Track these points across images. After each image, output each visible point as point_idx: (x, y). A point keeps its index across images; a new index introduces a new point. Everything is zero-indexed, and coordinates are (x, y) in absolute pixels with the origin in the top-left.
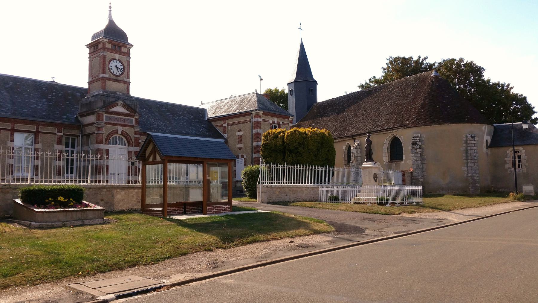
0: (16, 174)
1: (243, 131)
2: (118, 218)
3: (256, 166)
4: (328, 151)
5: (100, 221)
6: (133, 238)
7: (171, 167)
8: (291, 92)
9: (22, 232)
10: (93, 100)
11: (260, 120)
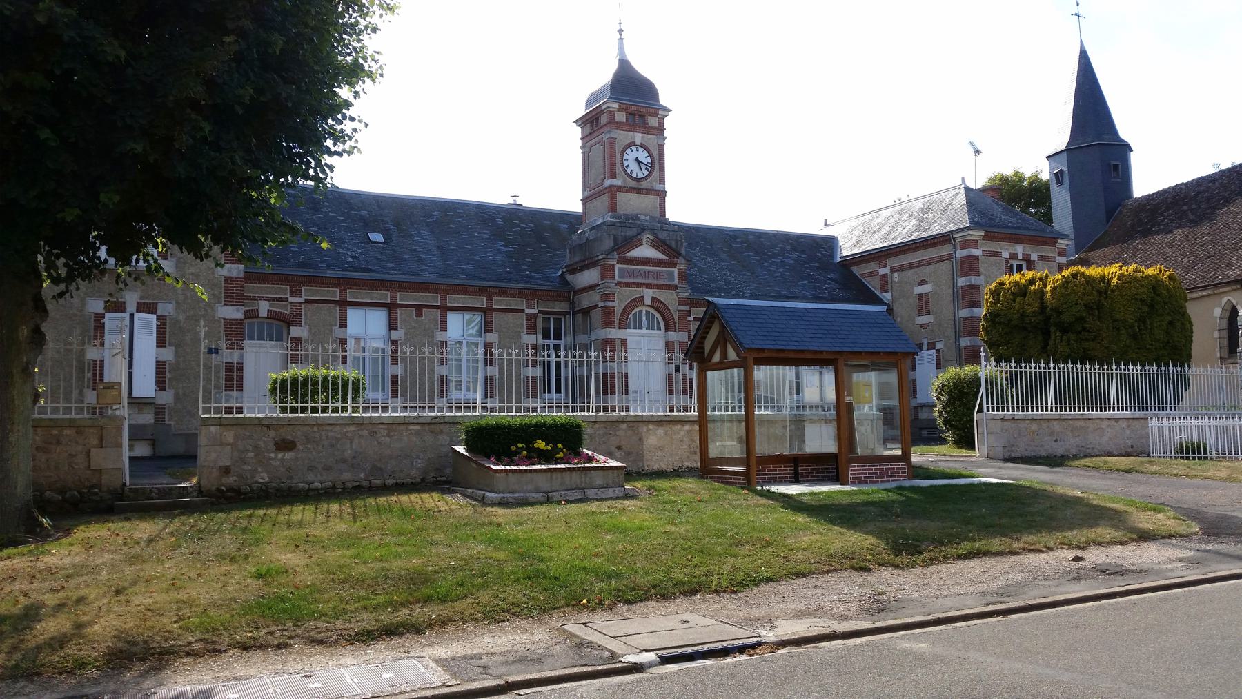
0: (454, 395)
1: (935, 283)
2: (653, 488)
3: (968, 370)
4: (1171, 323)
5: (618, 492)
6: (687, 531)
7: (762, 373)
8: (1058, 176)
9: (468, 512)
10: (592, 235)
11: (977, 252)
